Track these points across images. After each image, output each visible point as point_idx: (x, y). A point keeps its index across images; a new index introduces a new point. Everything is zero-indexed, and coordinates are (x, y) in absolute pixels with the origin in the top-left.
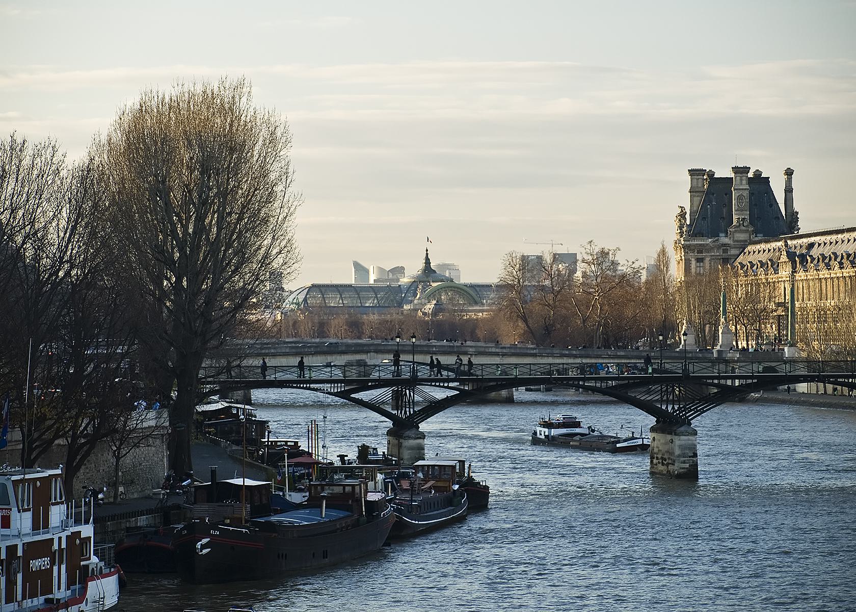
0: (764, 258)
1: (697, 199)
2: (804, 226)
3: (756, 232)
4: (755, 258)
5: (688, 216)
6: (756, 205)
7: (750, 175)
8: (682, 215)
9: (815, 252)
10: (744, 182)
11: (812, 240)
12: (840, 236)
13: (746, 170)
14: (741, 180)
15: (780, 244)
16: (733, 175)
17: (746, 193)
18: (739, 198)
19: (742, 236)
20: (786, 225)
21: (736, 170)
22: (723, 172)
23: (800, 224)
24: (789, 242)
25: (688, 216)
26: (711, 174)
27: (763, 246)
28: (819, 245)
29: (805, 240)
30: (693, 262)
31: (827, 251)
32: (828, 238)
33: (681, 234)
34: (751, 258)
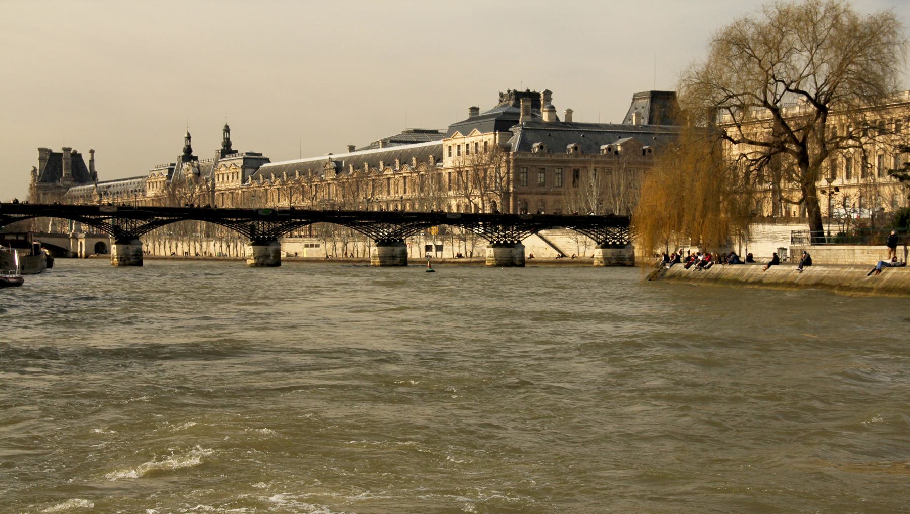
3: (75, 181)
8: (35, 171)
9: (111, 189)
13: (69, 149)
15: (93, 186)
16: (62, 152)
17: (70, 161)
18: (66, 163)
19: (68, 183)
20: (93, 177)
21: (64, 149)
22: (57, 149)
26: (50, 151)
27: (80, 187)
30: (42, 195)
31: (119, 189)
33: (35, 180)
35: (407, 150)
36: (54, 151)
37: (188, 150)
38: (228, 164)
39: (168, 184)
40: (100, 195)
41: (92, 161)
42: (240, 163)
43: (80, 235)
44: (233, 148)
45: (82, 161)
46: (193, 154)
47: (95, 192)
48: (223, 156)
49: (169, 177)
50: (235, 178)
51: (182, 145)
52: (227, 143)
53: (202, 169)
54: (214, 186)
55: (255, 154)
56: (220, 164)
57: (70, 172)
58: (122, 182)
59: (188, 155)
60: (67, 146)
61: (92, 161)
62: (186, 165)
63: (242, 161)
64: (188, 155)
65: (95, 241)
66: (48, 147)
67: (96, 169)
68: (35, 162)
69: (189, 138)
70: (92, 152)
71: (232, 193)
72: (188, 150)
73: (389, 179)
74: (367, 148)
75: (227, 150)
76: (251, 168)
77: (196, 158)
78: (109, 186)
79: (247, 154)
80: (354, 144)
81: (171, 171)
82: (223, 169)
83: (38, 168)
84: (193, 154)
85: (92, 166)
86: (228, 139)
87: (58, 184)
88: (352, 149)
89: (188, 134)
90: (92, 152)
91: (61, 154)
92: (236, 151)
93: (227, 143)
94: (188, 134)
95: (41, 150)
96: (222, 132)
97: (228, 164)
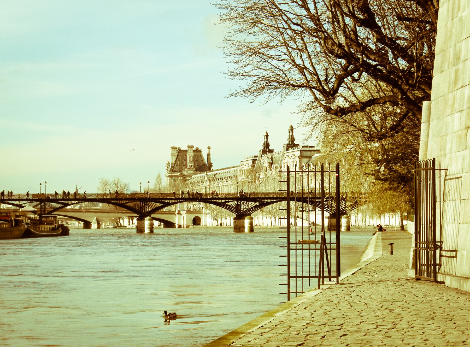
0: (199, 179)
1: (174, 158)
2: (214, 168)
4: (195, 180)
5: (170, 165)
8: (168, 164)
10: (192, 151)
12: (227, 170)
13: (192, 147)
16: (187, 149)
18: (190, 157)
20: (207, 167)
22: (184, 147)
27: (199, 175)
32: (222, 171)
34: (194, 180)
37: (267, 145)
38: (290, 155)
39: (252, 171)
40: (209, 180)
41: (209, 155)
42: (298, 154)
43: (182, 212)
46: (271, 148)
47: (206, 179)
48: (287, 150)
49: (253, 166)
51: (262, 141)
52: (292, 139)
53: (274, 159)
55: (310, 147)
56: (285, 156)
57: (193, 164)
58: (225, 171)
59: (267, 149)
60: (191, 145)
61: (209, 155)
62: (264, 157)
63: (299, 152)
64: (267, 149)
65: (193, 216)
67: (212, 161)
69: (267, 136)
70: (209, 148)
75: (291, 145)
76: (306, 157)
77: (272, 151)
79: (303, 147)
81: (254, 161)
82: (287, 159)
84: (271, 148)
85: (209, 159)
86: (292, 136)
90: (209, 148)
91: (187, 150)
92: (298, 145)
94: (267, 133)
95: (173, 148)
97: (290, 155)
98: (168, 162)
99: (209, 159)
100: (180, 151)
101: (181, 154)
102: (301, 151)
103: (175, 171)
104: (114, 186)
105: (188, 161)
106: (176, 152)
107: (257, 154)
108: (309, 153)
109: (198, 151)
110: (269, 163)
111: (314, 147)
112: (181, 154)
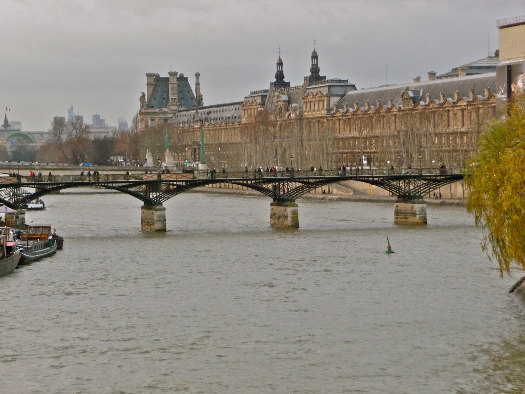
1: (151, 89)
2: (206, 103)
6: (181, 92)
7: (178, 76)
10: (175, 80)
11: (210, 109)
13: (176, 74)
14: (173, 79)
16: (169, 76)
17: (176, 86)
18: (173, 88)
19: (174, 108)
21: (171, 74)
22: (164, 75)
23: (204, 101)
24: (199, 111)
25: (146, 97)
28: (214, 112)
29: (207, 110)
32: (219, 109)
35: (482, 79)
36: (161, 76)
37: (280, 76)
38: (315, 91)
44: (321, 74)
45: (188, 85)
50: (321, 107)
52: (315, 70)
54: (302, 113)
55: (340, 81)
57: (176, 97)
59: (280, 81)
60: (173, 71)
64: (280, 81)
66: (155, 72)
68: (143, 88)
71: (318, 121)
72: (280, 76)
73: (463, 110)
74: (446, 76)
75: (315, 77)
76: (337, 95)
78: (210, 112)
79: (332, 81)
80: (435, 71)
83: (146, 94)
87: (165, 110)
88: (432, 75)
89: (280, 59)
91: (168, 78)
92: (324, 78)
93: (315, 70)
95: (149, 75)
96: (310, 58)
98: (143, 94)
99: (197, 90)
100: (158, 79)
101: (157, 83)
102: (329, 86)
103: (153, 107)
104: (71, 128)
105: (170, 92)
106: (152, 80)
107: (267, 87)
108: (340, 89)
109: (183, 80)
110: (284, 101)
111: (347, 81)
112: (157, 83)
